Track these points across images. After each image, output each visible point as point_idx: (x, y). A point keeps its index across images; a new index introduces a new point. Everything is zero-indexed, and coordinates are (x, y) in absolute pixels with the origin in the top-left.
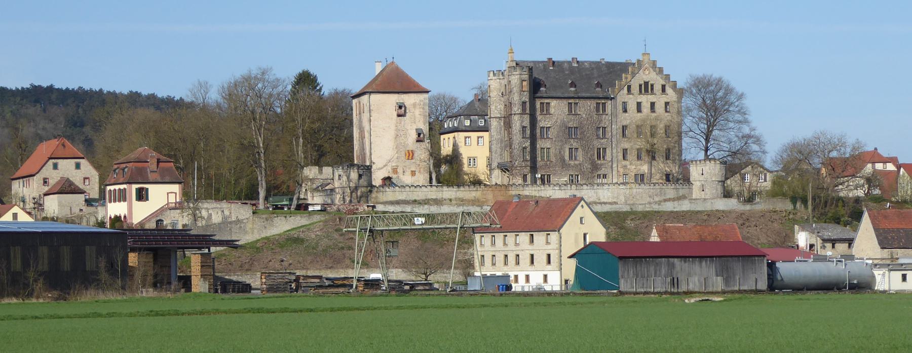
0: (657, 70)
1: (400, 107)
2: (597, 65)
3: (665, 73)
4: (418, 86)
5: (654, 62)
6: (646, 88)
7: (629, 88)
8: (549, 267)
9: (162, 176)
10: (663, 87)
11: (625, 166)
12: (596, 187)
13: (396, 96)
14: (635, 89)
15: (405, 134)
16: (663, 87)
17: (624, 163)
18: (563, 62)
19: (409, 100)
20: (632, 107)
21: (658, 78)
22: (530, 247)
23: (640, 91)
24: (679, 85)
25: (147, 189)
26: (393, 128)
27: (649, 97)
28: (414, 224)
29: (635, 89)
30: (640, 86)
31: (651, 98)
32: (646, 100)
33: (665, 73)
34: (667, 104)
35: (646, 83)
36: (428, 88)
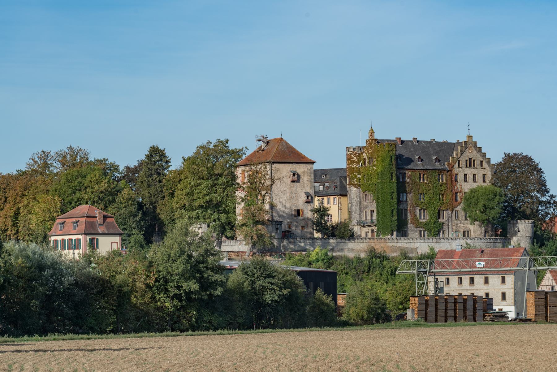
0: (478, 149)
1: (294, 175)
2: (431, 143)
3: (483, 151)
4: (303, 157)
5: (476, 142)
6: (470, 163)
7: (459, 162)
8: (504, 303)
9: (108, 229)
10: (482, 162)
11: (457, 225)
12: (450, 241)
13: (291, 165)
14: (463, 164)
15: (297, 197)
16: (482, 162)
17: (456, 221)
18: (408, 141)
19: (300, 169)
20: (460, 178)
21: (478, 155)
22: (485, 287)
23: (466, 166)
24: (492, 162)
25: (97, 239)
26: (288, 191)
27: (472, 170)
28: (476, 267)
29: (463, 164)
30: (466, 161)
31: (474, 171)
32: (470, 172)
33: (483, 151)
34: (484, 175)
35: (470, 159)
36: (314, 160)
